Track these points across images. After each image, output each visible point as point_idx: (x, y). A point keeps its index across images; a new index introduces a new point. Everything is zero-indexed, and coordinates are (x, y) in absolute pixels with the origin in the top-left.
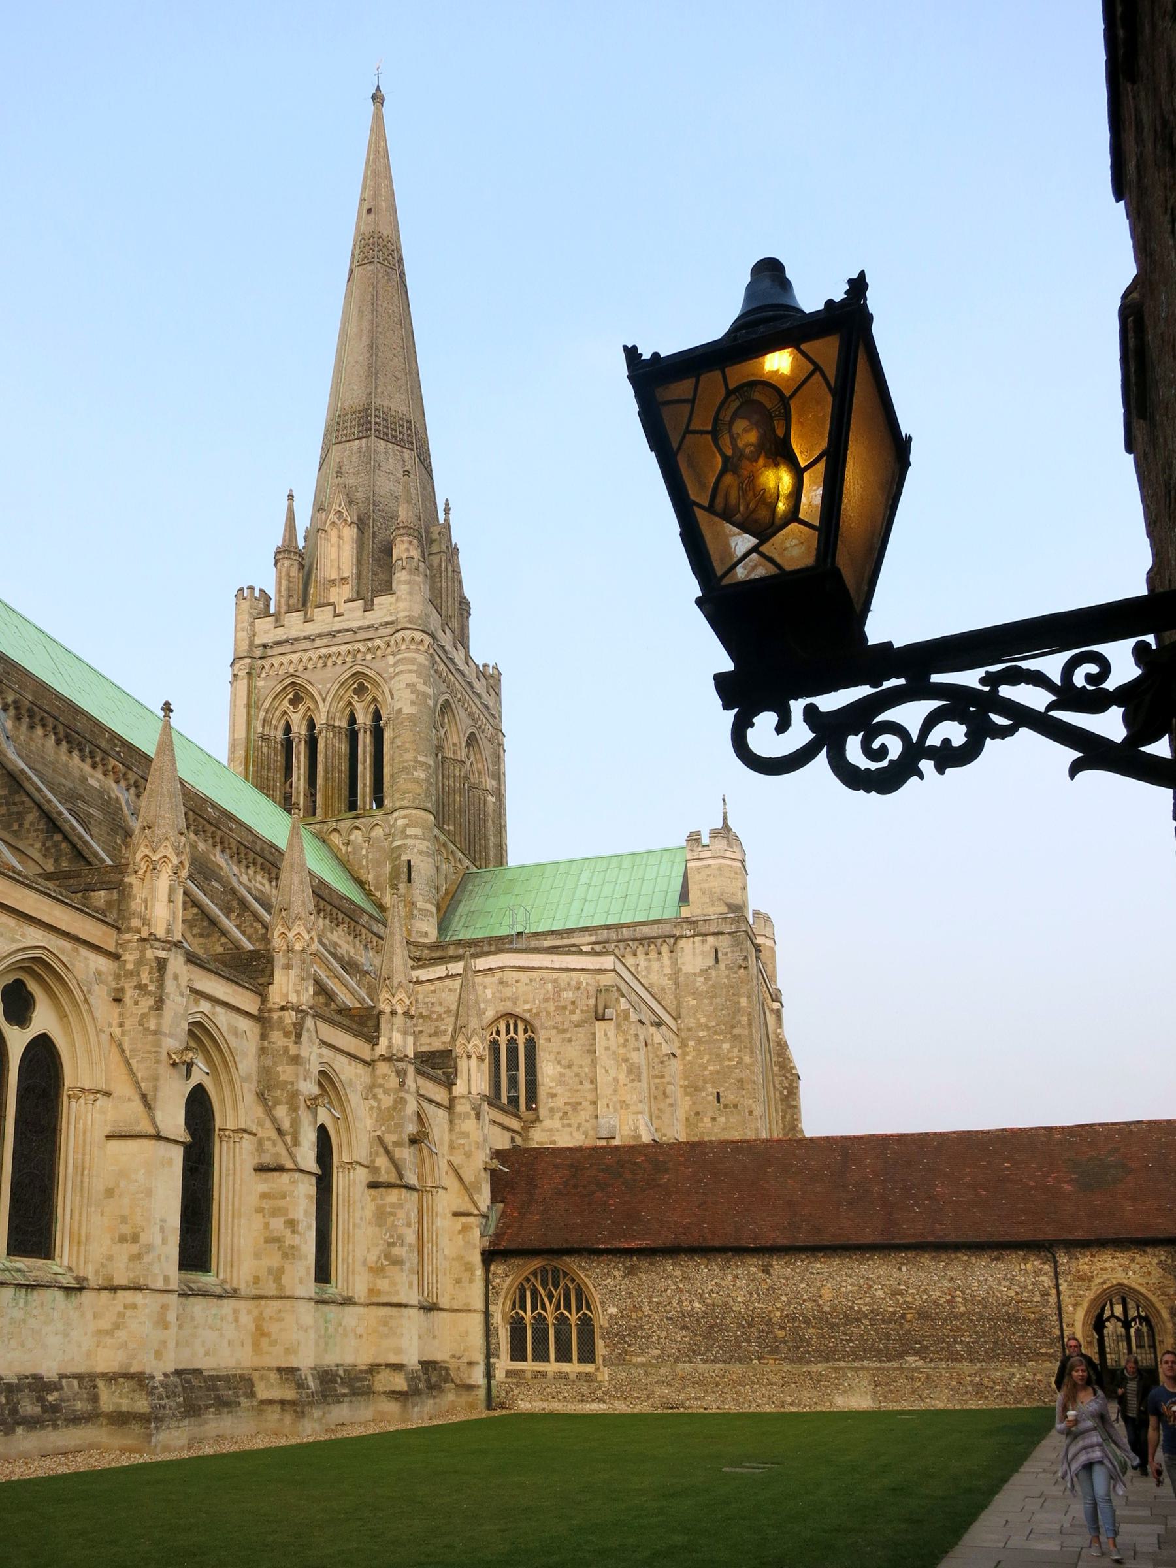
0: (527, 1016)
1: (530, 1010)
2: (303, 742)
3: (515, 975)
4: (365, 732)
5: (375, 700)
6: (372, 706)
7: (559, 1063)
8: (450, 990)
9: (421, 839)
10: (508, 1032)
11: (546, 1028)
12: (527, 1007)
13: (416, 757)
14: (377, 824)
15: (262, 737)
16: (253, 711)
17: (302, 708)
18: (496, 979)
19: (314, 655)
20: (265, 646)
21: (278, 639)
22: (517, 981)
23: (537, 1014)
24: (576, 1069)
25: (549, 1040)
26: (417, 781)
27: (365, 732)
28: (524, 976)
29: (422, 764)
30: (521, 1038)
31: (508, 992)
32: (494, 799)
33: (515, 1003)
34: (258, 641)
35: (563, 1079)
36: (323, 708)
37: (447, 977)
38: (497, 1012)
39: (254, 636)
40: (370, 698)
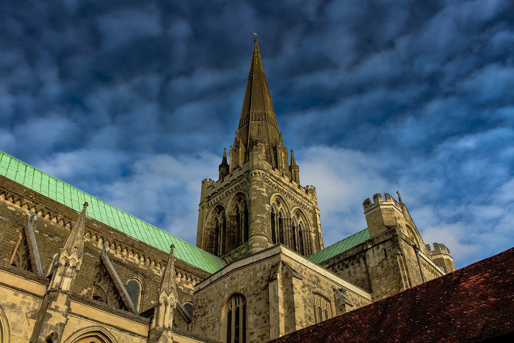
0: (242, 292)
1: (243, 289)
2: (222, 227)
3: (237, 272)
4: (242, 215)
5: (245, 201)
6: (244, 204)
7: (255, 313)
8: (211, 290)
9: (259, 247)
10: (236, 305)
12: (242, 287)
14: (244, 248)
17: (221, 214)
18: (229, 278)
19: (224, 193)
21: (213, 192)
23: (246, 289)
24: (263, 315)
25: (251, 302)
27: (242, 215)
28: (241, 272)
30: (241, 306)
31: (234, 282)
32: (315, 235)
35: (257, 322)
37: (211, 283)
38: (229, 294)
40: (243, 201)
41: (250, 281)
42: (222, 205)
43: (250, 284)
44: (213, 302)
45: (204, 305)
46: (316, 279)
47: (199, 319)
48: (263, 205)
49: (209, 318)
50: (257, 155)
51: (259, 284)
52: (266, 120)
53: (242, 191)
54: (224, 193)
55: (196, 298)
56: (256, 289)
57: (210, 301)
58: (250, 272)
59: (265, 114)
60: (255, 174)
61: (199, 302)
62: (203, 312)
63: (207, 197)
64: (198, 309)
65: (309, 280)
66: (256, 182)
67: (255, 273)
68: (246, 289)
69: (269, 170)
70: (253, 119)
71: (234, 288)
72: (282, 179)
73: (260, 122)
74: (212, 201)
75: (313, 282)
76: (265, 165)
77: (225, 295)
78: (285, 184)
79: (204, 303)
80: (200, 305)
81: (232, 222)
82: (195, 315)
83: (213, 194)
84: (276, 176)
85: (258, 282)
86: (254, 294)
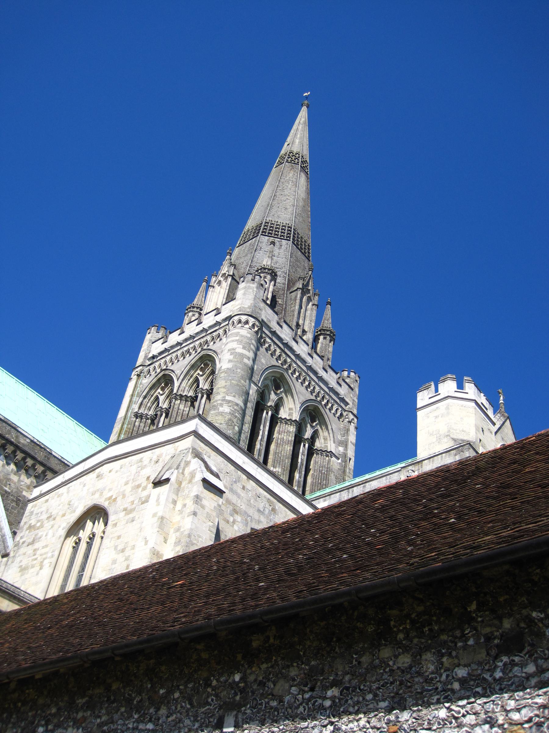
1: (110, 498)
11: (116, 513)
12: (109, 495)
13: (225, 397)
15: (137, 415)
16: (134, 399)
19: (179, 353)
20: (154, 357)
22: (110, 471)
26: (221, 414)
29: (229, 402)
33: (101, 494)
34: (150, 355)
35: (114, 566)
36: (176, 384)
39: (149, 353)
41: (126, 483)
42: (171, 375)
43: (125, 491)
44: (54, 519)
45: (38, 524)
46: (267, 506)
47: (22, 550)
48: (243, 382)
49: (38, 549)
50: (251, 290)
51: (140, 489)
52: (290, 237)
53: (210, 353)
54: (179, 353)
55: (31, 510)
56: (131, 499)
57: (48, 518)
58: (131, 466)
59: (291, 228)
60: (240, 322)
61: (33, 517)
62: (33, 536)
63: (150, 358)
64: (27, 530)
65: (249, 504)
66: (237, 338)
67: (140, 468)
68: (115, 500)
69: (270, 321)
70: (265, 232)
71: (97, 495)
72: (293, 344)
73: (279, 240)
74: (157, 364)
75: (259, 511)
76: (264, 311)
77: (77, 507)
78: (298, 356)
79: (38, 521)
80: (33, 522)
81: (182, 407)
82: (19, 541)
83: (161, 353)
84: (282, 336)
85: (139, 486)
86: (125, 510)
